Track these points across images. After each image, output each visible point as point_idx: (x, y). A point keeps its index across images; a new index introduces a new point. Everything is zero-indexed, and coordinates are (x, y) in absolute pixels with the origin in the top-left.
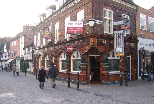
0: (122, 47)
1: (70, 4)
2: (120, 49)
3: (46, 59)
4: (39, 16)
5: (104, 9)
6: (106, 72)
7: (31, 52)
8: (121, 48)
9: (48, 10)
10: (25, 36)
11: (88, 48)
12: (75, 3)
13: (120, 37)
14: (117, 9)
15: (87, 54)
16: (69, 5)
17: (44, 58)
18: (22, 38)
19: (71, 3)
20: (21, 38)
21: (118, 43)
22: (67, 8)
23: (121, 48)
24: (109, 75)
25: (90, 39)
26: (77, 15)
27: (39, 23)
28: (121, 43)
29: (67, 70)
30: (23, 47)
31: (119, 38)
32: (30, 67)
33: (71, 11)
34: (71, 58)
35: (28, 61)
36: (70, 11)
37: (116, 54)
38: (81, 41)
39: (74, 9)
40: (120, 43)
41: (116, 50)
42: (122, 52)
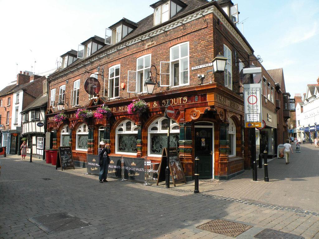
0: (259, 112)
1: (153, 31)
2: (256, 116)
3: (78, 133)
4: (63, 56)
5: (224, 45)
6: (226, 156)
7: (41, 119)
8: (257, 114)
9: (91, 43)
10: (25, 91)
11: (199, 111)
12: (166, 30)
13: (255, 95)
14: (235, 50)
15: (193, 123)
16: (150, 34)
17: (73, 130)
18: (18, 95)
19: (157, 30)
20: (15, 95)
21: (252, 105)
22: (143, 39)
23: (258, 115)
24: (231, 160)
25: (206, 95)
26: (169, 52)
27: (65, 66)
28: (257, 106)
29: (140, 152)
30: (20, 110)
31: (253, 96)
32: (36, 145)
33: (152, 44)
34: (148, 130)
35: (31, 135)
36: (150, 43)
37: (247, 124)
38: (180, 98)
39: (161, 41)
40: (255, 104)
41: (248, 117)
42: (258, 120)
